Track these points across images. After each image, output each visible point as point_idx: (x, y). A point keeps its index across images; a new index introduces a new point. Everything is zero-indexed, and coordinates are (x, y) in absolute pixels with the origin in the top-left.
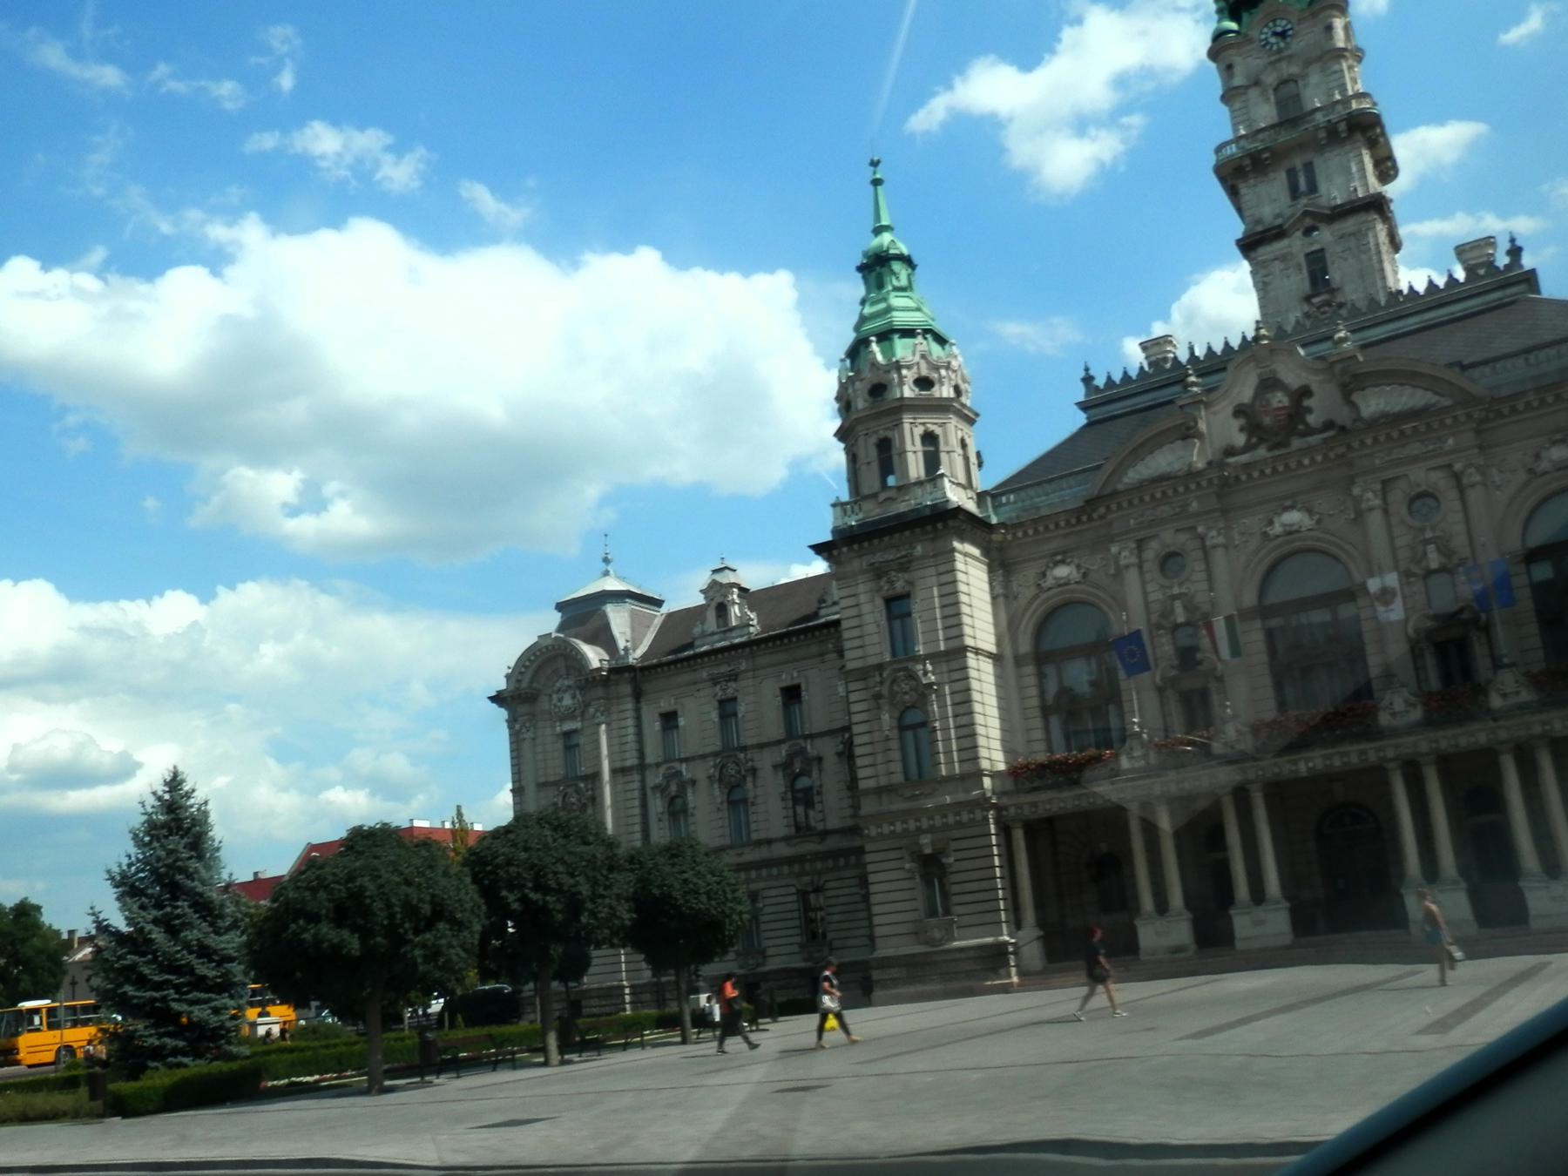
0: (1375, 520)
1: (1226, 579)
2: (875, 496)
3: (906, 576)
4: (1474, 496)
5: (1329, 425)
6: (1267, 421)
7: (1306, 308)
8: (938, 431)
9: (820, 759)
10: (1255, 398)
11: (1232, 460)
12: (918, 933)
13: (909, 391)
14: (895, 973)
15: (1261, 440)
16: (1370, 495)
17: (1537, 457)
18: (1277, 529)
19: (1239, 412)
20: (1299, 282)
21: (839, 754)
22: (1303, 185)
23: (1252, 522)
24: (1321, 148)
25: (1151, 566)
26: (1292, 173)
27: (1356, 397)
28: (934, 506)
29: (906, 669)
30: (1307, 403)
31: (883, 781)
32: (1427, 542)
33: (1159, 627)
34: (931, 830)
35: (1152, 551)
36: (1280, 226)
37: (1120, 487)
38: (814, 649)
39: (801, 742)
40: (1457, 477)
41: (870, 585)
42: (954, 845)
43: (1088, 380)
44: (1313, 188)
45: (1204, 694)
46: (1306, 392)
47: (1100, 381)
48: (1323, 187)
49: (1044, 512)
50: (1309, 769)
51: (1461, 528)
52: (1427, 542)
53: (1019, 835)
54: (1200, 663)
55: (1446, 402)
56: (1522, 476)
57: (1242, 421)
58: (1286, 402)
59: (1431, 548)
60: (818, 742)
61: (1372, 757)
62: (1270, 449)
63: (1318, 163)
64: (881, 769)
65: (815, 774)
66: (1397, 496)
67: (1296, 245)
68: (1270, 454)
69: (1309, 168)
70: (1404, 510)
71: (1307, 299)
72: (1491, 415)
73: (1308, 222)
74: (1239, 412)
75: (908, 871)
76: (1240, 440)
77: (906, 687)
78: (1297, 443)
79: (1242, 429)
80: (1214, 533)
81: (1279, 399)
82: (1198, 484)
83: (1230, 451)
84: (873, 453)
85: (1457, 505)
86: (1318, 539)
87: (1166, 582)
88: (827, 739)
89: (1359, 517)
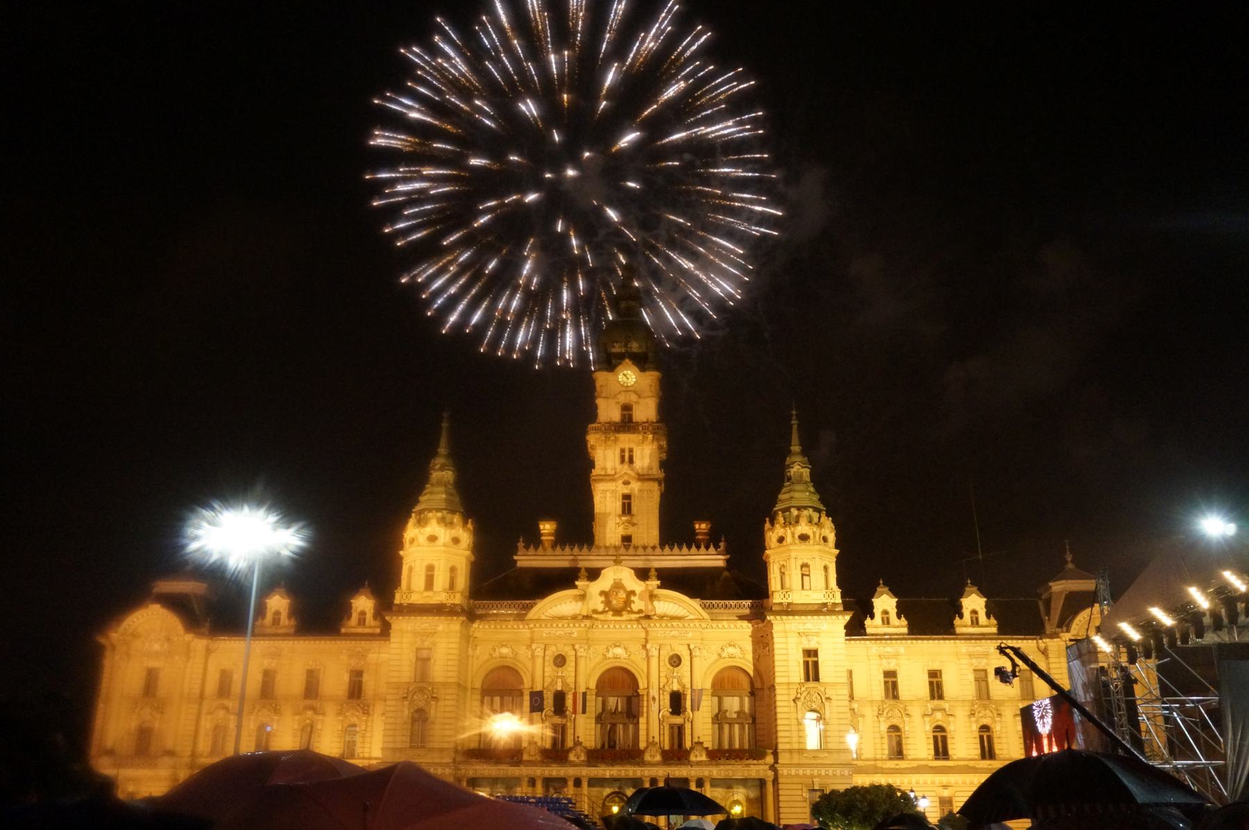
5: (640, 611)
6: (614, 602)
19: (603, 593)
26: (623, 451)
27: (656, 603)
35: (552, 651)
37: (543, 617)
44: (631, 461)
46: (633, 593)
56: (715, 657)
57: (603, 598)
58: (624, 596)
61: (639, 774)
69: (631, 451)
73: (626, 478)
76: (601, 607)
83: (595, 611)
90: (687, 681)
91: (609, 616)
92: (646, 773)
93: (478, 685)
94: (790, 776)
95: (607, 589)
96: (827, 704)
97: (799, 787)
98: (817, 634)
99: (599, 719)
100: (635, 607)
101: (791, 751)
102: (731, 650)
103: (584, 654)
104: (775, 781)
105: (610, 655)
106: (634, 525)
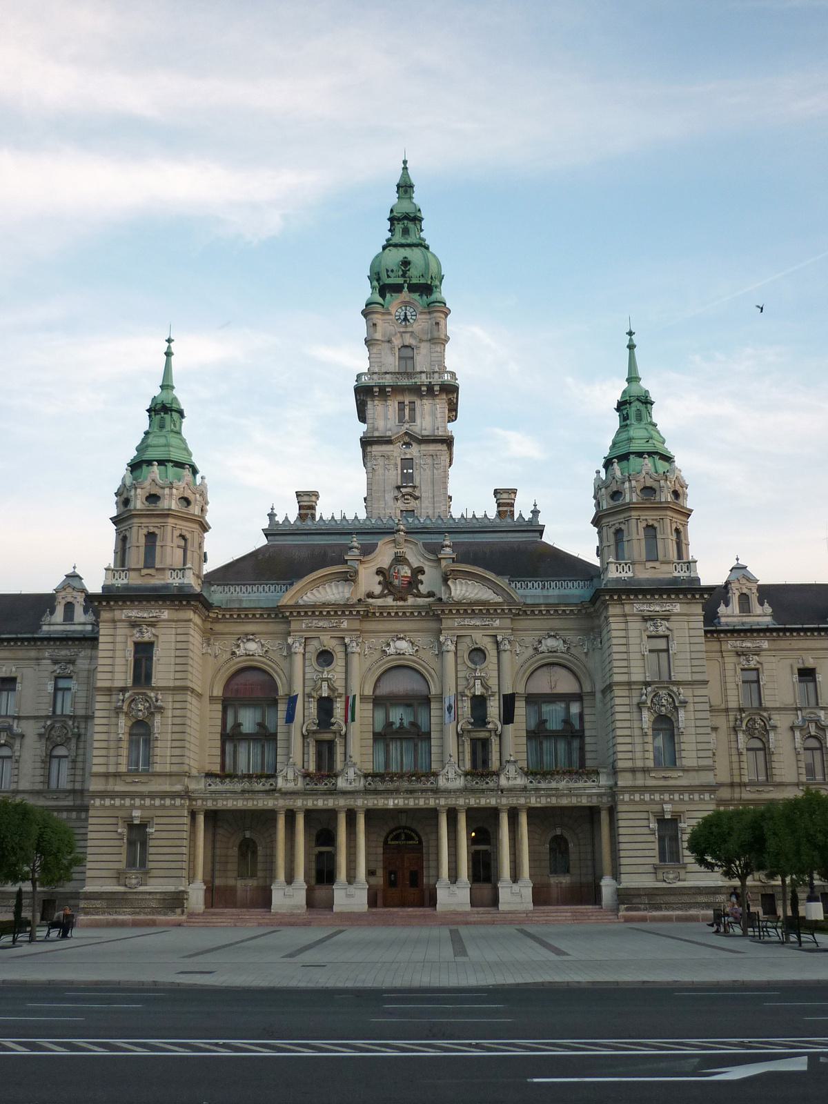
0: (450, 658)
1: (358, 674)
2: (139, 570)
3: (154, 630)
4: (506, 657)
5: (431, 594)
6: (396, 582)
7: (396, 493)
8: (188, 536)
9: (22, 736)
10: (390, 567)
11: (370, 600)
12: (119, 877)
13: (174, 505)
14: (98, 904)
15: (391, 593)
16: (449, 643)
17: (540, 642)
18: (391, 650)
19: (380, 572)
20: (394, 476)
21: (40, 735)
22: (406, 414)
23: (377, 641)
24: (421, 396)
25: (312, 656)
28: (181, 587)
29: (144, 694)
30: (420, 577)
31: (112, 769)
32: (476, 678)
33: (310, 696)
34: (142, 807)
35: (314, 646)
36: (390, 437)
37: (301, 602)
38: (33, 654)
39: (10, 720)
40: (497, 643)
41: (127, 631)
42: (156, 820)
43: (272, 516)
45: (331, 744)
46: (421, 571)
47: (280, 519)
48: (418, 421)
49: (245, 605)
50: (394, 804)
51: (495, 674)
52: (476, 678)
53: (201, 819)
54: (333, 724)
55: (501, 600)
56: (530, 651)
57: (380, 578)
59: (478, 682)
60: (24, 723)
61: (432, 803)
62: (394, 600)
63: (418, 403)
64: (112, 760)
65: (17, 746)
66: (465, 647)
67: (397, 451)
68: (394, 603)
70: (466, 656)
71: (398, 488)
72: (521, 613)
73: (407, 439)
74: (380, 572)
75: (120, 834)
76: (377, 589)
77: (141, 707)
78: (411, 600)
79: (380, 583)
80: (354, 644)
81: (406, 571)
82: (351, 612)
83: (370, 595)
84: (142, 541)
85: (495, 660)
86: (415, 662)
87: (320, 669)
88: (32, 722)
89: (441, 654)
90: (493, 683)
91: (389, 601)
92: (442, 802)
93: (218, 691)
94: (632, 801)
95: (386, 566)
96: (681, 713)
97: (644, 815)
98: (666, 617)
99: (377, 737)
100: (423, 589)
101: (633, 771)
102: (551, 643)
103: (358, 650)
104: (612, 811)
105: (391, 650)
106: (416, 498)
